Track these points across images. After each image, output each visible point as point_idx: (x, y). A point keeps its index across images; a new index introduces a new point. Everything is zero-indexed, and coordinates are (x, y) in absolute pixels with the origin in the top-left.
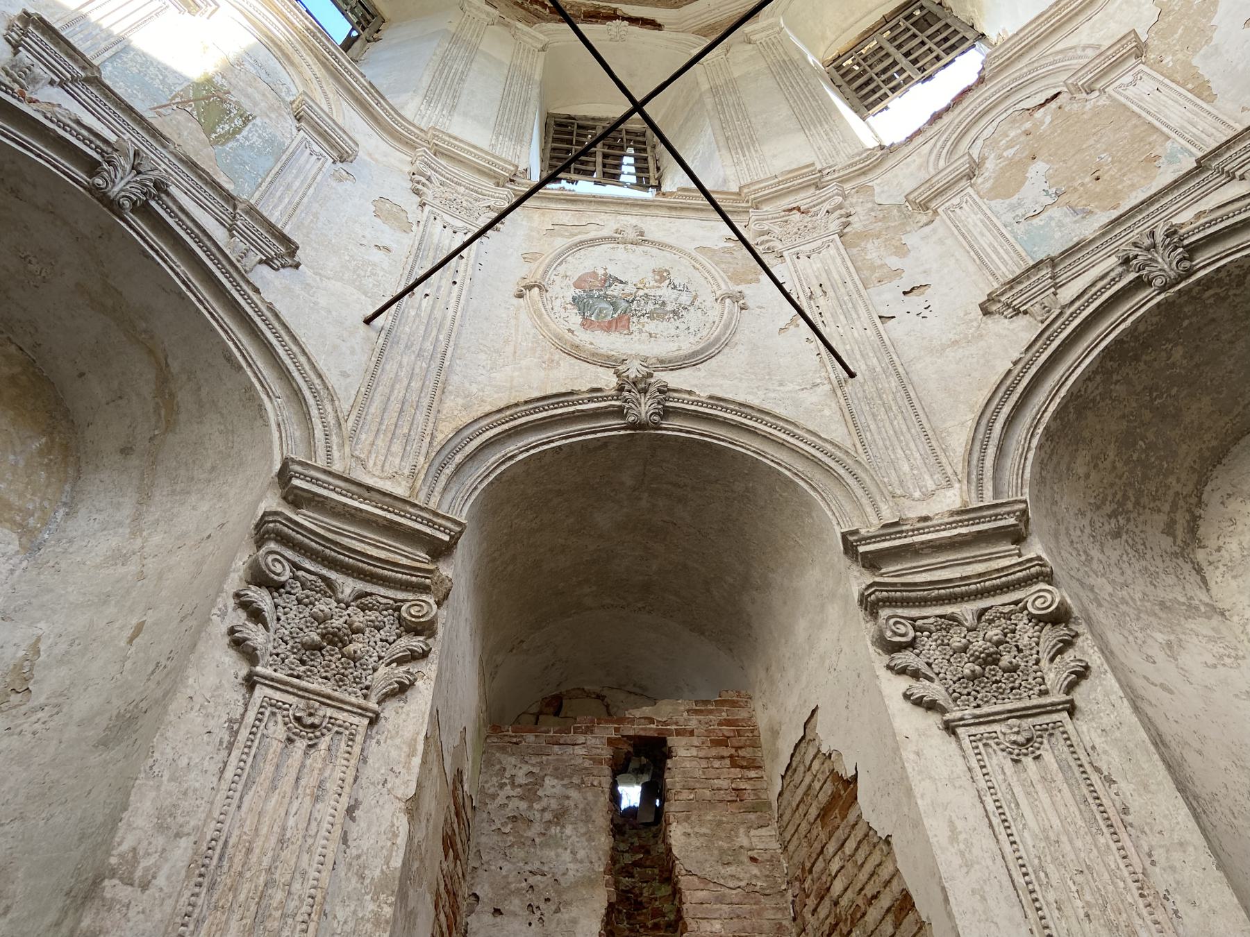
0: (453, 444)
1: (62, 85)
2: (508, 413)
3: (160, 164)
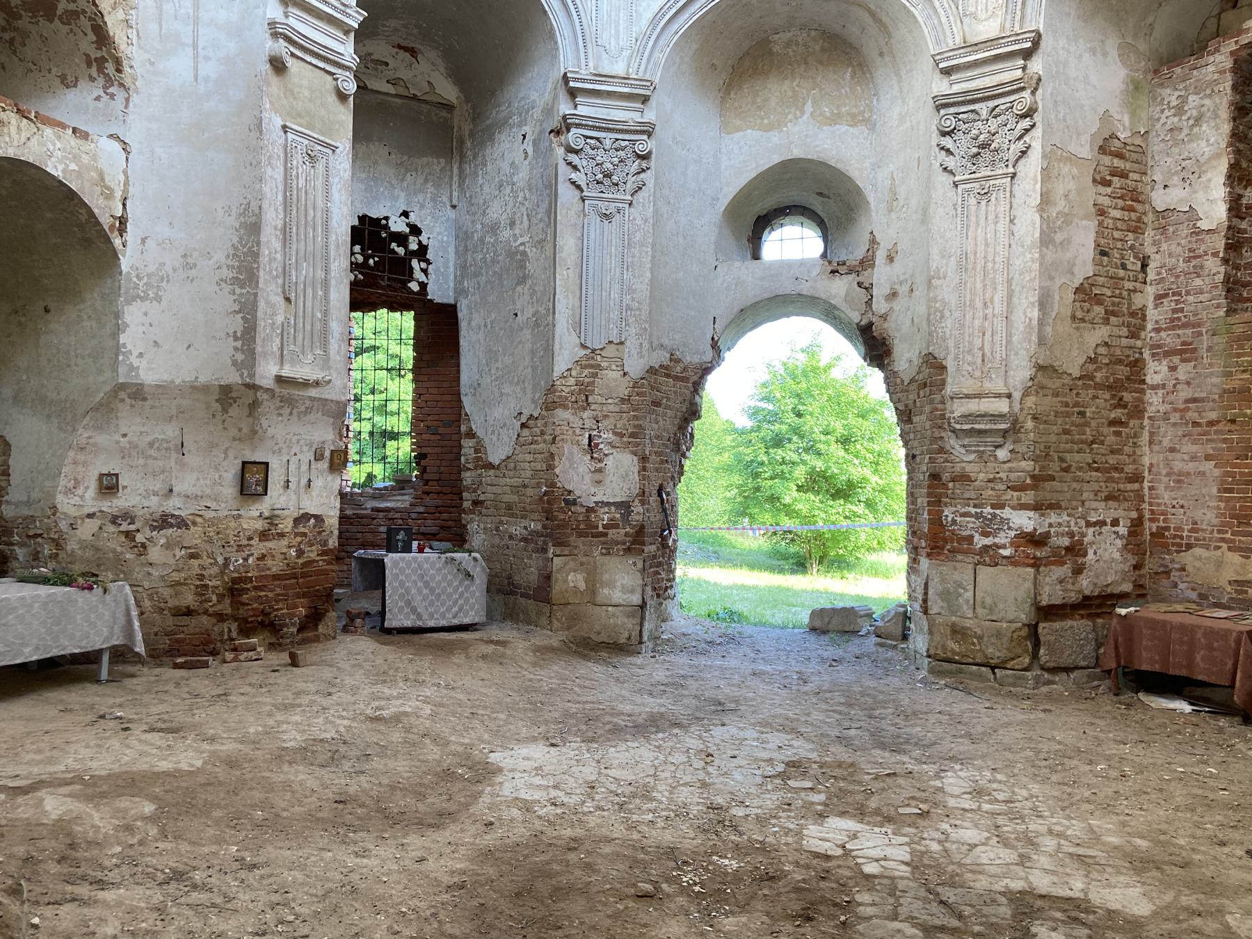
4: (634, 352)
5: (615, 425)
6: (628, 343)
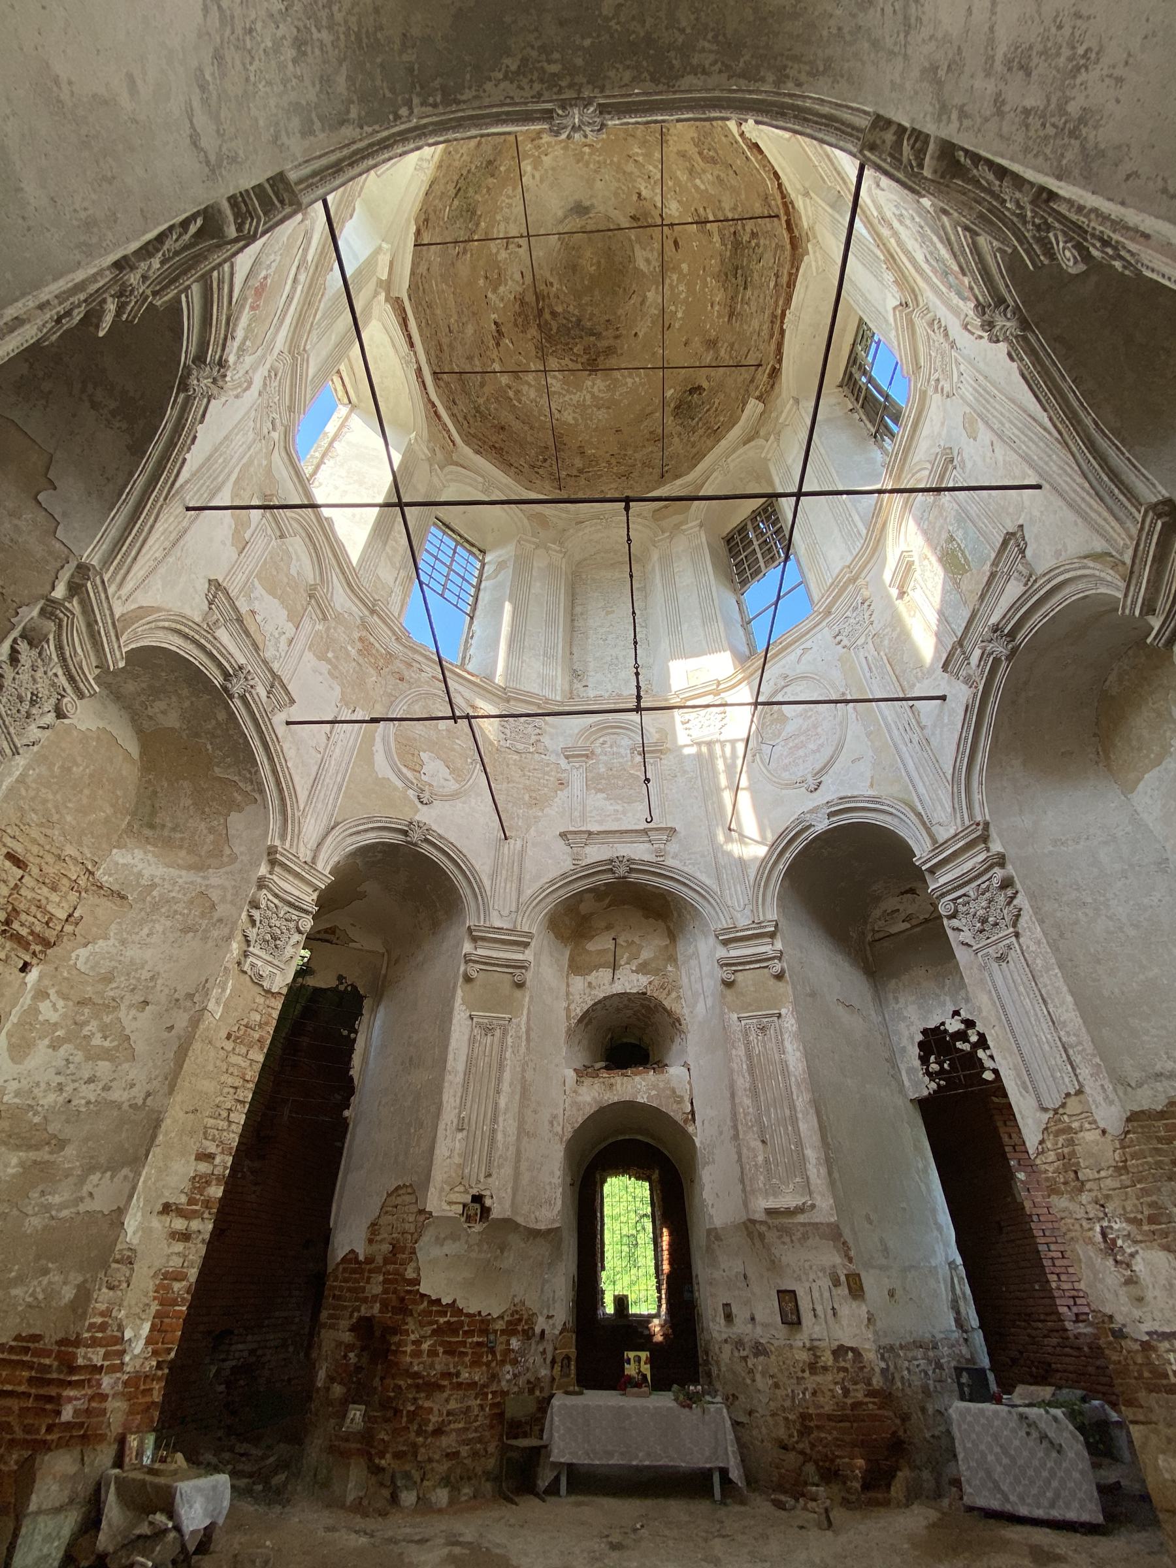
0: (1095, 483)
1: (967, 658)
2: (1059, 425)
3: (981, 629)
4: (1100, 1099)
5: (1124, 1208)
6: (1087, 1089)
